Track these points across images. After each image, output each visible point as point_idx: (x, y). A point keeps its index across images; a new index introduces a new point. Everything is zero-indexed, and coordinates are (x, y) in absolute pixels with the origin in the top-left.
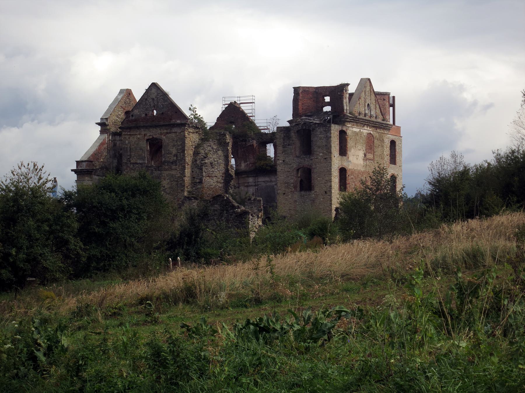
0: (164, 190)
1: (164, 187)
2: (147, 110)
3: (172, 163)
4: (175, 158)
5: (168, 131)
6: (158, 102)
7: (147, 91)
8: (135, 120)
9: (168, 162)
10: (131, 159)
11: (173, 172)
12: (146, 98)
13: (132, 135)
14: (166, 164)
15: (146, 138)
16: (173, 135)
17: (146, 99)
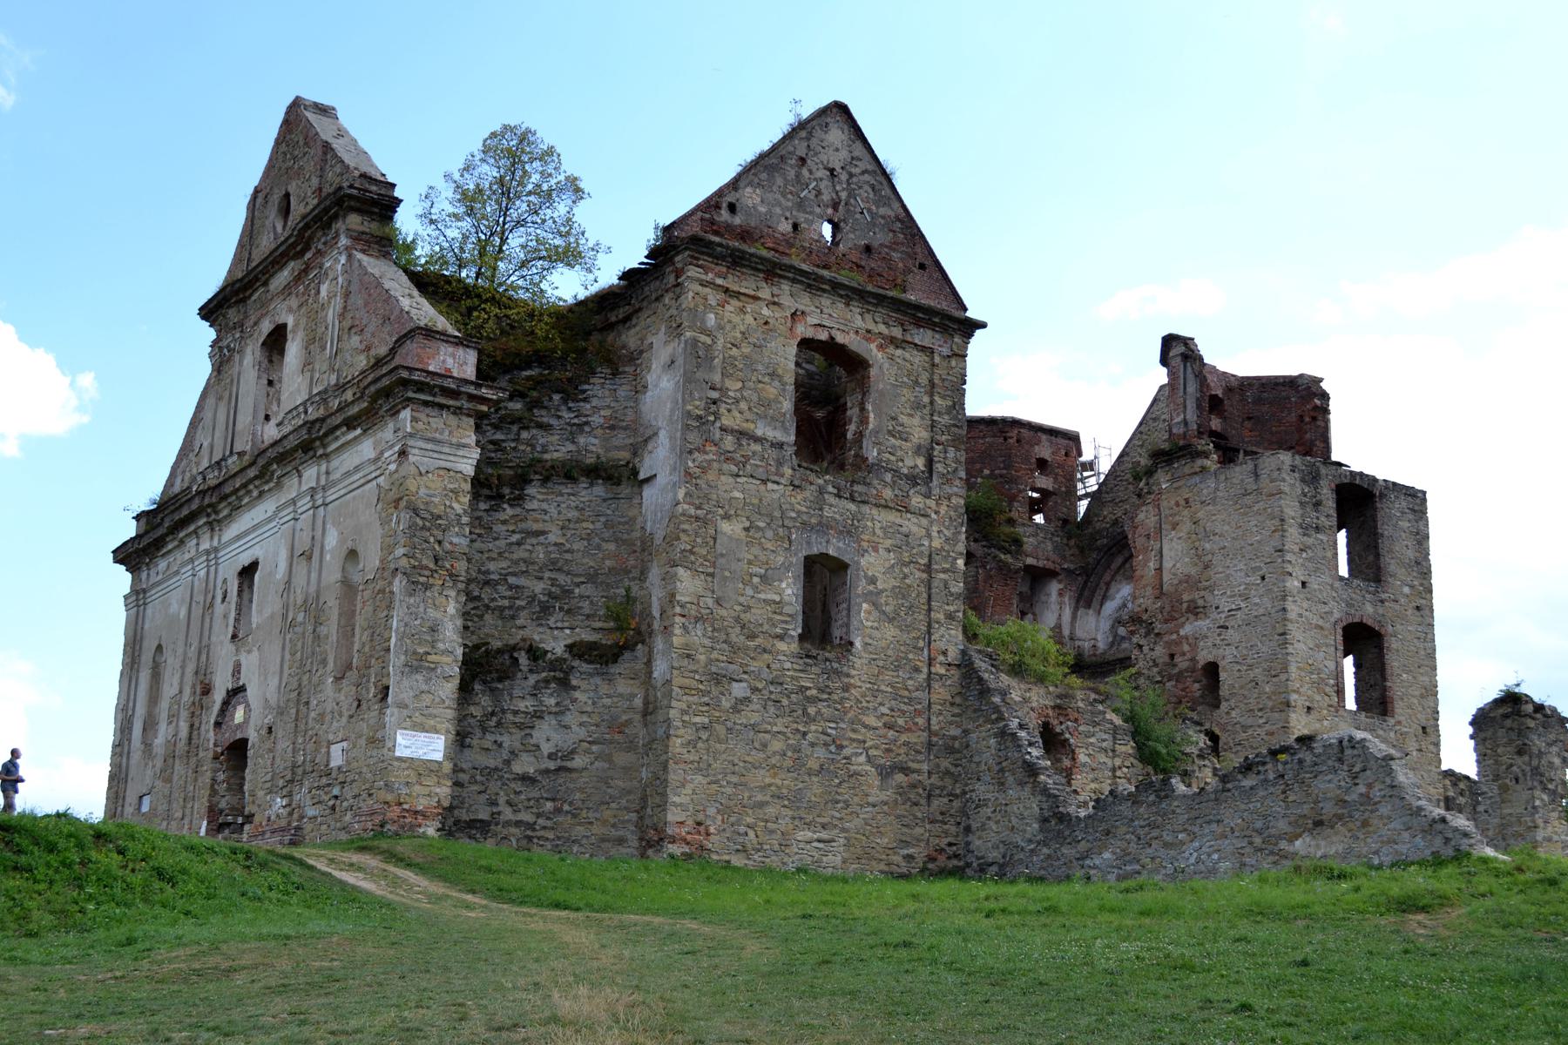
0: (873, 598)
1: (873, 580)
2: (801, 205)
3: (913, 479)
4: (921, 462)
5: (897, 332)
6: (852, 195)
7: (802, 129)
8: (745, 234)
9: (896, 472)
10: (723, 410)
11: (911, 524)
12: (801, 152)
13: (737, 295)
14: (888, 477)
15: (802, 330)
16: (918, 359)
17: (803, 160)
